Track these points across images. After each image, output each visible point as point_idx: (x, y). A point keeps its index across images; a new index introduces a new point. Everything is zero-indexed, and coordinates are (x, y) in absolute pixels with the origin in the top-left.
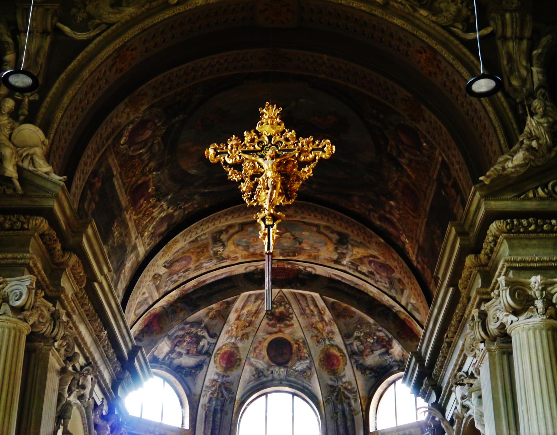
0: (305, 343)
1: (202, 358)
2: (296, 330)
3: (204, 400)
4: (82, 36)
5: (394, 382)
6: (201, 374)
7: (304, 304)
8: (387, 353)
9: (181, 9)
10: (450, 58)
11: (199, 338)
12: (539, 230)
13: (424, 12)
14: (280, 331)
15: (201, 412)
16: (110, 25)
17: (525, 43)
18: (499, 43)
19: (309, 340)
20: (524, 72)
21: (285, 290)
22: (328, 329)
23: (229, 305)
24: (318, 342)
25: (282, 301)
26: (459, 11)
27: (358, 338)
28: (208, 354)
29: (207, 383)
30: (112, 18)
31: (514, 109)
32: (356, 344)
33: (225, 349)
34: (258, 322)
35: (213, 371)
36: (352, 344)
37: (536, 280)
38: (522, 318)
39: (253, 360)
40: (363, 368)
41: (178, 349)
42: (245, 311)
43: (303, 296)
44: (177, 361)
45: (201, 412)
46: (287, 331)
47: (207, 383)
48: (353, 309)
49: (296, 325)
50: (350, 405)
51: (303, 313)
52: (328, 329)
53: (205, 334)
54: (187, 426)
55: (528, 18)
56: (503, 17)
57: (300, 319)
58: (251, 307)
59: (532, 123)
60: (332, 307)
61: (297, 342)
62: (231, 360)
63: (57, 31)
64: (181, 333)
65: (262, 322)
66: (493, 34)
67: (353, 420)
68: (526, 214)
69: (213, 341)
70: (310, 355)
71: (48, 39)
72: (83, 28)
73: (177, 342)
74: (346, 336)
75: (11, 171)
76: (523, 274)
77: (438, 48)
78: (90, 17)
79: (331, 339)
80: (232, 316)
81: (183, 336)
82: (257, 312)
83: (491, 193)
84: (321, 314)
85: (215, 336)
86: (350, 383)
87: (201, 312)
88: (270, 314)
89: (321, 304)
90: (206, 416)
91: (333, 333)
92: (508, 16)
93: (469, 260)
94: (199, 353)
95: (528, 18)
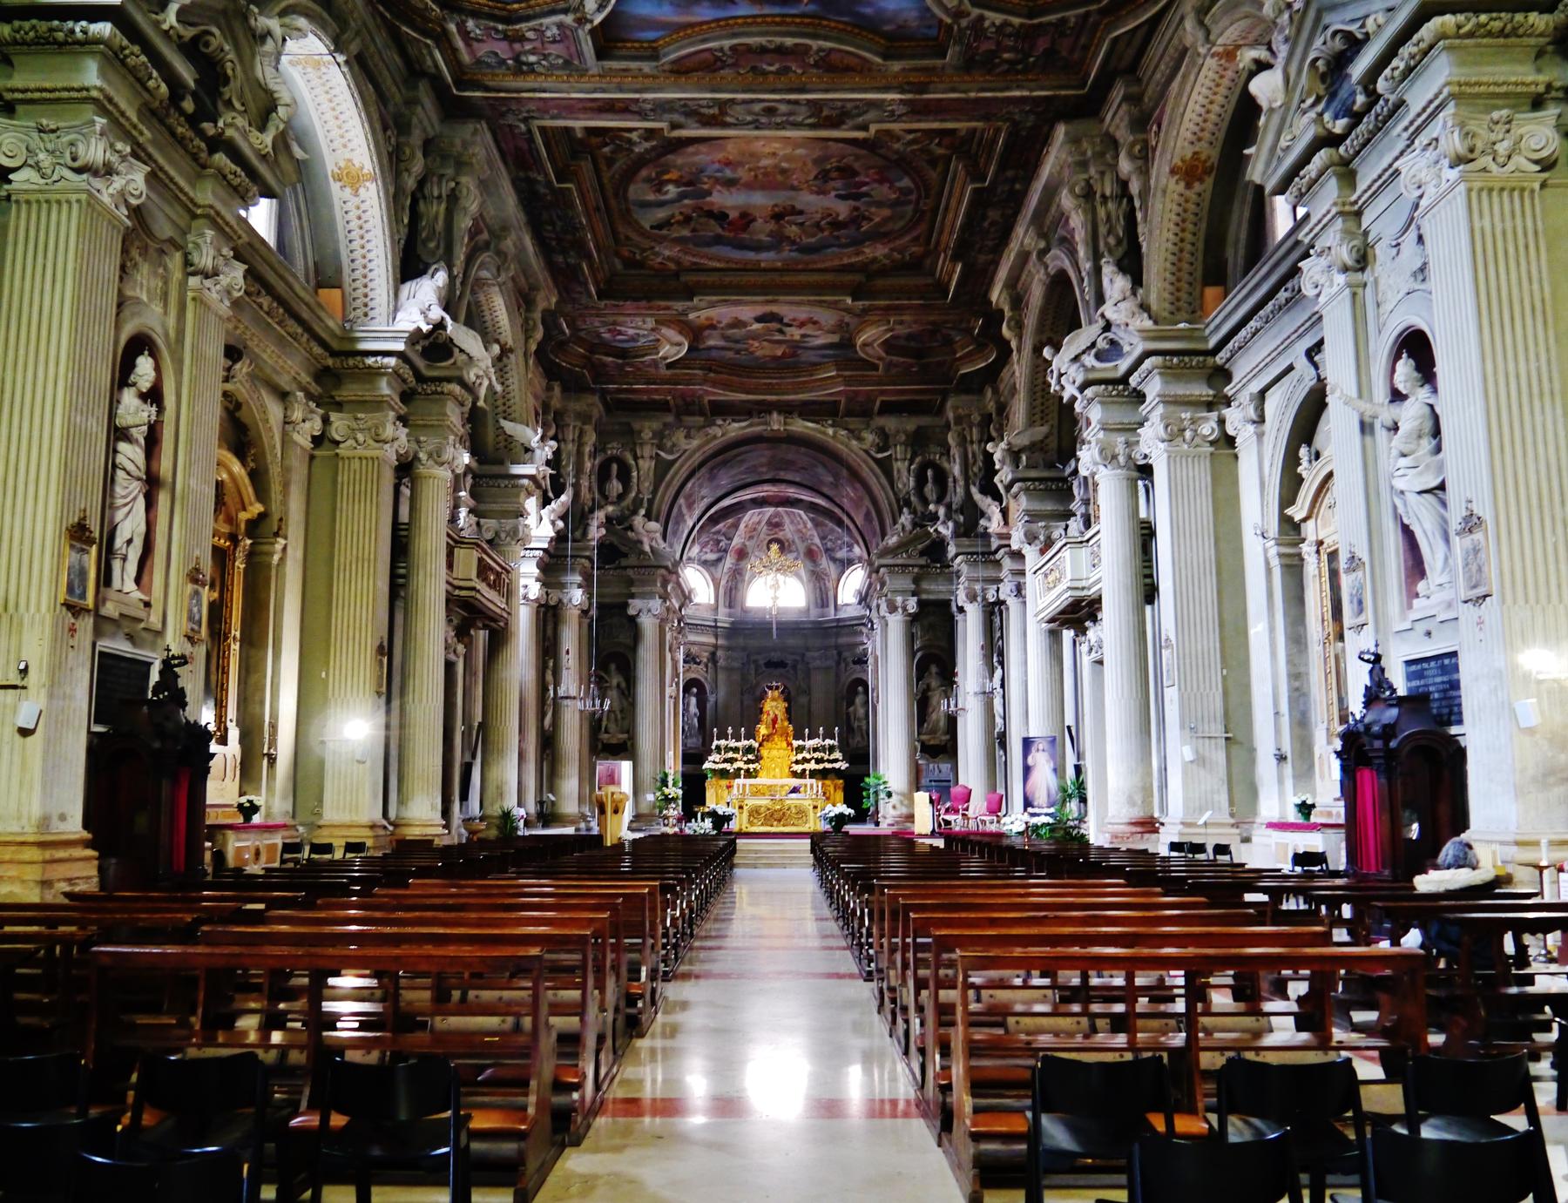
2: (788, 532)
3: (723, 583)
4: (670, 457)
11: (719, 542)
13: (854, 442)
23: (739, 520)
25: (777, 515)
28: (726, 551)
31: (898, 501)
35: (729, 561)
37: (899, 599)
40: (834, 560)
45: (721, 591)
54: (712, 601)
58: (756, 519)
60: (812, 520)
62: (742, 554)
65: (763, 528)
72: (671, 452)
73: (704, 546)
74: (823, 538)
75: (647, 548)
80: (742, 526)
83: (882, 555)
85: (731, 539)
87: (720, 526)
88: (769, 523)
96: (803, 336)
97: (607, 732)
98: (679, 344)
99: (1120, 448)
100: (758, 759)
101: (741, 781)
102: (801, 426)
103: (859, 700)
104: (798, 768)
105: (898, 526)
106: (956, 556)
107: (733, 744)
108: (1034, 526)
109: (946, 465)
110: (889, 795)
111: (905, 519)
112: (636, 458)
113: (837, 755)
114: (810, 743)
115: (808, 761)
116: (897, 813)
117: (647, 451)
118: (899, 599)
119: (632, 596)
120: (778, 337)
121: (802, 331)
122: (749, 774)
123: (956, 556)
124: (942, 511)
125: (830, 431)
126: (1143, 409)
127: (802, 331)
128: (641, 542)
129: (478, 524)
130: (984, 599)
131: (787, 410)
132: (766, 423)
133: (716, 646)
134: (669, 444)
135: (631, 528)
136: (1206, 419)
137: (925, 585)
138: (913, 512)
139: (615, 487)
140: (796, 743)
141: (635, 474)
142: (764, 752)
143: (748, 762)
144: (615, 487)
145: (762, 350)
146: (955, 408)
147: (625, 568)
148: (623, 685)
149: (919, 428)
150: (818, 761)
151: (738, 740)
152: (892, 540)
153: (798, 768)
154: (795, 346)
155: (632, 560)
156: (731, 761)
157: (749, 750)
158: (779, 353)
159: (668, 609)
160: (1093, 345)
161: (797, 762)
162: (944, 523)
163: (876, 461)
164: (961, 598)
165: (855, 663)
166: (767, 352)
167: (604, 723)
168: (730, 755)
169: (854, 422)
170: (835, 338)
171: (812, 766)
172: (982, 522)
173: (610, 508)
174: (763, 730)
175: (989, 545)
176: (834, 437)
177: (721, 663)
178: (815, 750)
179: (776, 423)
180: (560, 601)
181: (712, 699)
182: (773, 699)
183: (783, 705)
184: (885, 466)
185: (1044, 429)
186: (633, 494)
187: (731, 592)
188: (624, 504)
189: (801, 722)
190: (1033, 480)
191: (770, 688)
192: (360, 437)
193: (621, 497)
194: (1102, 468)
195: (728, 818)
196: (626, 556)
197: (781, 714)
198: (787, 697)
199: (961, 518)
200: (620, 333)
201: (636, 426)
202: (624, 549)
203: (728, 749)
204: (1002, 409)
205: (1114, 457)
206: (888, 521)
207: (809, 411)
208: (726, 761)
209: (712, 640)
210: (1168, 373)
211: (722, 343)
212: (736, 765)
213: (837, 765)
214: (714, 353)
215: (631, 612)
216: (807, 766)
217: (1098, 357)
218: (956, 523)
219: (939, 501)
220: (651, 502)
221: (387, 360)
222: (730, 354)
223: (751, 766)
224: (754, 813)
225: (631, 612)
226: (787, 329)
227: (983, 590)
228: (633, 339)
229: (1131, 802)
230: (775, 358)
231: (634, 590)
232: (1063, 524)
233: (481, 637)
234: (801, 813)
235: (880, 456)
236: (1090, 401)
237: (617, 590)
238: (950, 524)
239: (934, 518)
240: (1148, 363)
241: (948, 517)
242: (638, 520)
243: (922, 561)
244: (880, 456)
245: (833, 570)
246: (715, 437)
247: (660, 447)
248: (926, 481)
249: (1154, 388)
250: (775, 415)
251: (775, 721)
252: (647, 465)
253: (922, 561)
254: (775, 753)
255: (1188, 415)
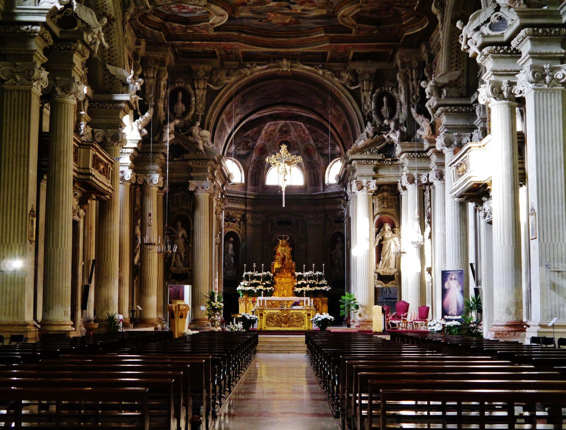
0: (297, 143)
1: (249, 151)
5: (337, 161)
6: (250, 157)
7: (296, 127)
8: (334, 149)
9: (250, 77)
10: (344, 97)
11: (247, 143)
12: (367, 164)
13: (336, 79)
14: (285, 137)
15: (249, 174)
16: (226, 84)
17: (370, 93)
18: (361, 92)
19: (298, 142)
20: (369, 104)
21: (287, 122)
22: (307, 137)
23: (261, 129)
24: (303, 143)
25: (286, 125)
26: (349, 78)
27: (321, 142)
29: (252, 161)
30: (227, 81)
32: (320, 145)
33: (260, 146)
34: (275, 134)
35: (254, 156)
36: (318, 144)
38: (360, 191)
39: (272, 150)
41: (238, 148)
42: (269, 130)
43: (296, 124)
44: (238, 153)
45: (249, 174)
46: (288, 138)
47: (252, 161)
48: (319, 130)
49: (292, 135)
50: (317, 171)
51: (296, 130)
52: (307, 137)
53: (251, 140)
54: (243, 182)
55: (372, 84)
56: (363, 82)
57: (295, 133)
58: (272, 128)
59: (367, 129)
60: (309, 129)
61: (293, 142)
63: (208, 86)
64: (240, 141)
65: (277, 133)
66: (360, 87)
67: (318, 177)
68: (364, 159)
69: (254, 143)
70: (299, 149)
71: (206, 91)
73: (237, 145)
74: (315, 141)
75: (201, 148)
76: (362, 177)
77: (341, 93)
78: (219, 80)
79: (308, 142)
80: (263, 132)
81: (241, 143)
82: (274, 130)
83: (353, 153)
84: (304, 132)
85: (255, 141)
86: (317, 161)
87: (249, 132)
88: (281, 130)
89: (304, 127)
90: (252, 176)
91: (310, 139)
92: (365, 83)
93: (348, 166)
94: (248, 149)
95: (372, 84)
96: (303, 10)
97: (175, 266)
98: (222, 15)
99: (505, 87)
100: (273, 284)
101: (261, 298)
102: (302, 68)
103: (338, 246)
104: (298, 290)
105: (364, 134)
106: (401, 154)
107: (256, 274)
108: (450, 135)
109: (396, 94)
110: (357, 307)
111: (369, 129)
112: (194, 89)
113: (324, 282)
114: (306, 274)
115: (305, 285)
116: (363, 319)
117: (202, 85)
118: (364, 181)
119: (192, 178)
120: (287, 11)
121: (302, 7)
122: (267, 294)
123: (401, 154)
124: (392, 125)
125: (321, 72)
126: (520, 61)
127: (302, 7)
128: (197, 144)
129: (92, 132)
130: (419, 181)
131: (293, 58)
132: (279, 67)
133: (245, 211)
134: (216, 80)
135: (191, 134)
136: (465, 136)
137: (381, 172)
138: (374, 125)
139: (181, 107)
140: (297, 274)
141: (193, 99)
142: (277, 280)
143: (266, 286)
144: (181, 107)
145: (276, 19)
146: (402, 58)
147: (187, 160)
148: (186, 236)
149: (378, 70)
150: (312, 285)
151: (260, 272)
152: (360, 143)
153: (298, 290)
154: (298, 17)
155: (191, 155)
156: (255, 285)
157: (267, 278)
158: (287, 21)
159: (215, 187)
160: (489, 20)
161: (298, 286)
162: (394, 132)
163: (350, 91)
164: (404, 181)
165: (336, 222)
166: (279, 21)
167: (173, 262)
168: (255, 281)
169: (336, 66)
170: (324, 12)
171: (308, 288)
172: (418, 132)
173: (177, 122)
174: (277, 265)
175: (423, 147)
176: (323, 76)
177: (249, 221)
178: (310, 278)
179: (285, 66)
180: (145, 181)
181: (243, 245)
182: (283, 246)
183: (288, 249)
184: (356, 95)
185: (458, 73)
186: (192, 112)
187: (256, 172)
188: (187, 118)
189: (300, 260)
190: (450, 105)
191: (281, 238)
192: (18, 78)
193: (185, 114)
194: (493, 99)
195: (253, 322)
196: (187, 152)
197: (287, 255)
198: (291, 244)
199: (405, 129)
200: (184, 8)
201: (194, 67)
202: (186, 148)
203: (253, 277)
204: (432, 58)
205: (501, 92)
206: (358, 129)
207: (306, 59)
208: (251, 285)
209: (243, 207)
210: (535, 38)
211: (250, 15)
212: (258, 288)
213: (324, 288)
214: (245, 21)
215: (192, 189)
216: (304, 289)
217: (491, 28)
218: (402, 133)
219: (391, 118)
220: (204, 117)
221: (34, 28)
222: (256, 22)
223: (268, 288)
224: (270, 318)
225: (192, 189)
226: (292, 6)
227: (419, 176)
228: (192, 12)
229: (509, 312)
230: (285, 25)
231: (192, 174)
232: (469, 134)
233: (93, 204)
234: (300, 318)
235: (353, 88)
236: (486, 56)
237: (182, 175)
238: (398, 133)
239: (387, 128)
240: (522, 33)
241: (397, 128)
242: (196, 130)
243: (380, 157)
244: (353, 88)
245: (322, 161)
246: (246, 76)
247: (210, 82)
248: (383, 105)
249: (526, 48)
250: (285, 62)
251: (283, 259)
252: (201, 93)
253: (380, 157)
254: (283, 280)
255: (456, 134)
